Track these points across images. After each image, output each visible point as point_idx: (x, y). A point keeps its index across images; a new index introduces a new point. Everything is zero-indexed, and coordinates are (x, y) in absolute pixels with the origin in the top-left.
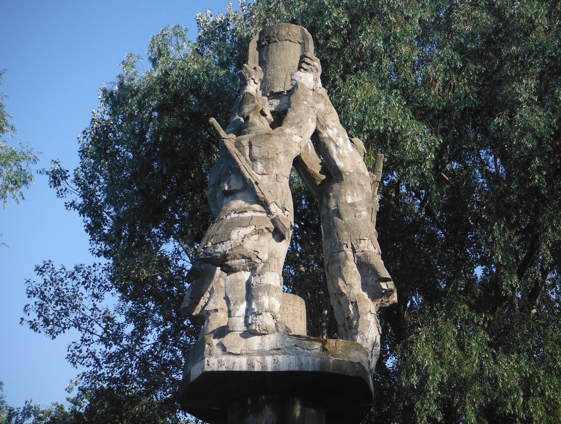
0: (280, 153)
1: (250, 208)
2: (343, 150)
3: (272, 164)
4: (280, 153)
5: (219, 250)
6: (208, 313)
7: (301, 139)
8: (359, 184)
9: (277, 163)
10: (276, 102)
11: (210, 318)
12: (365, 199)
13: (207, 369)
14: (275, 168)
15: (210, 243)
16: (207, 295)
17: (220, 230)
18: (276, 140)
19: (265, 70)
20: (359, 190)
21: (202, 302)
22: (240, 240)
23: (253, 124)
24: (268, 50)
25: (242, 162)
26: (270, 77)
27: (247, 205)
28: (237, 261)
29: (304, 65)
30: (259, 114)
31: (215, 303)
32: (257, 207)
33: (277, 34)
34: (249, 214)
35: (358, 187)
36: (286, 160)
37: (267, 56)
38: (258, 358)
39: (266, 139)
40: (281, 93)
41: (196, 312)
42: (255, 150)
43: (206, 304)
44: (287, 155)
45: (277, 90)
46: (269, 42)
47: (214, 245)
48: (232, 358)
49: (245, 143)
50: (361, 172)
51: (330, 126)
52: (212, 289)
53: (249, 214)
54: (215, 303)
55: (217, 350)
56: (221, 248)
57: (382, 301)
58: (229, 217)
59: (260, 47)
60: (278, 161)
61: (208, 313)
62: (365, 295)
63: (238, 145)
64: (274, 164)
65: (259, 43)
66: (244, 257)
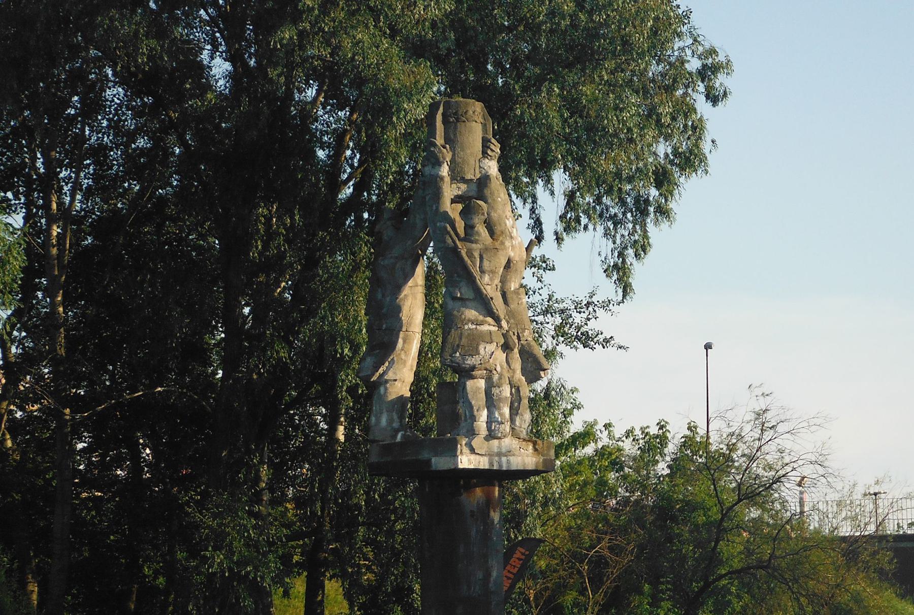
1: (486, 322)
5: (469, 362)
6: (387, 381)
10: (464, 187)
11: (388, 385)
13: (461, 466)
15: (458, 354)
16: (387, 364)
17: (463, 340)
19: (453, 149)
21: (381, 371)
22: (488, 357)
23: (478, 234)
24: (456, 128)
25: (476, 272)
26: (460, 160)
27: (481, 318)
28: (480, 372)
29: (489, 152)
31: (395, 373)
32: (489, 319)
33: (466, 113)
34: (485, 328)
37: (455, 135)
38: (496, 458)
39: (495, 254)
40: (471, 180)
41: (374, 378)
42: (486, 264)
43: (385, 373)
45: (469, 176)
46: (458, 120)
47: (463, 356)
48: (478, 456)
49: (477, 255)
52: (393, 359)
53: (485, 328)
54: (395, 373)
55: (466, 450)
56: (470, 361)
58: (466, 327)
59: (445, 121)
61: (387, 381)
63: (470, 254)
65: (444, 115)
66: (486, 369)
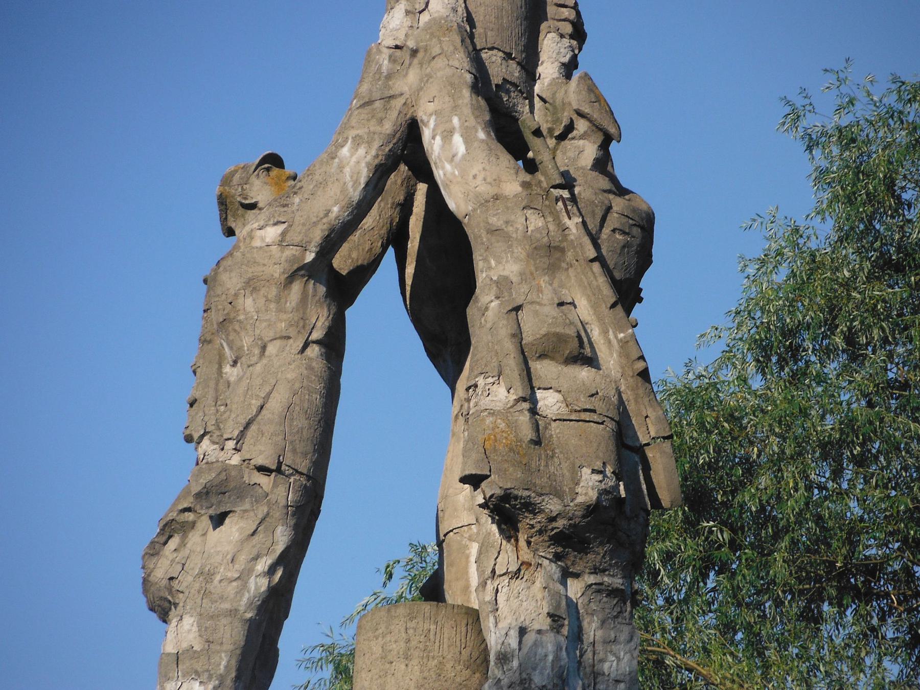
0: (236, 295)
2: (443, 168)
3: (235, 331)
4: (236, 295)
7: (280, 228)
8: (493, 231)
9: (240, 322)
12: (523, 255)
14: (243, 334)
18: (225, 270)
20: (499, 246)
30: (241, 211)
35: (493, 239)
36: (262, 301)
44: (255, 290)
50: (486, 196)
51: (425, 118)
57: (532, 526)
60: (242, 317)
62: (494, 528)
64: (237, 327)
